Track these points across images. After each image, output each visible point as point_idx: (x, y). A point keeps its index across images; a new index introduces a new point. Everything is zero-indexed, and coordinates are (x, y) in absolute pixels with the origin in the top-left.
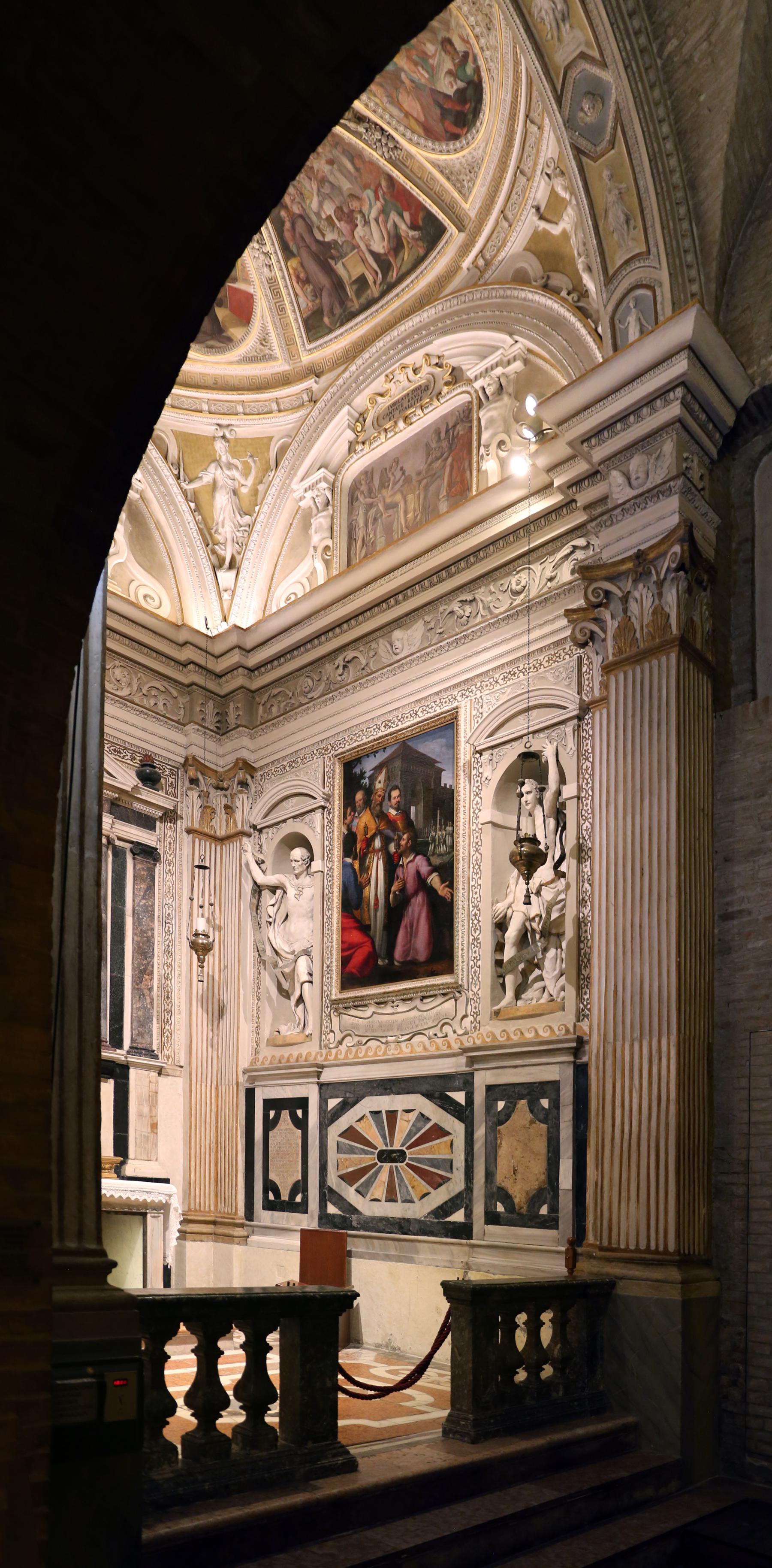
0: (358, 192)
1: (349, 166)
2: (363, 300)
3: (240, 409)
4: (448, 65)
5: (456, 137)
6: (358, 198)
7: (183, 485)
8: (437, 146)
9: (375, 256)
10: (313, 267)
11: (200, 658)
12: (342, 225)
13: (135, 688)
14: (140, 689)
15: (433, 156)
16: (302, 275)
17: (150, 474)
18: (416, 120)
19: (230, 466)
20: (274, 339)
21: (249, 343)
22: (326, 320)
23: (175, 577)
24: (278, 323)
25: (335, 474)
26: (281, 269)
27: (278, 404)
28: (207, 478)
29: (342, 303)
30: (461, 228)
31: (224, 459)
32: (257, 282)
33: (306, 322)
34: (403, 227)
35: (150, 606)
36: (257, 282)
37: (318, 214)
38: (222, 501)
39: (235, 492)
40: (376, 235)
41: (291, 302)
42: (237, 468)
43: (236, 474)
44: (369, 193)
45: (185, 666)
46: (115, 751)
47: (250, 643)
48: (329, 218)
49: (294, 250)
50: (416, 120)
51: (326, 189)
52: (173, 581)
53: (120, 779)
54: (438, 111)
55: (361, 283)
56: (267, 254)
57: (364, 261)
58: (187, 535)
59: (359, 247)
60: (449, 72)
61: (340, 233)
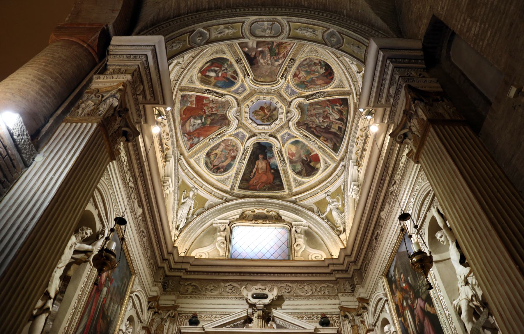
0: (324, 110)
1: (318, 106)
2: (343, 132)
3: (328, 184)
4: (319, 67)
5: (333, 78)
6: (325, 111)
7: (321, 216)
8: (331, 84)
9: (338, 120)
10: (326, 135)
11: (336, 268)
12: (327, 120)
13: (314, 290)
14: (316, 290)
15: (331, 87)
16: (325, 139)
17: (309, 219)
18: (323, 84)
19: (333, 202)
20: (328, 160)
21: (322, 165)
22: (338, 145)
23: (326, 246)
24: (327, 155)
25: (358, 182)
26: (319, 142)
27: (337, 176)
28: (328, 210)
29: (339, 137)
30: (349, 94)
31: (331, 201)
32: (316, 150)
33: (333, 149)
34: (339, 107)
35: (318, 259)
36: (316, 150)
37: (320, 123)
38: (334, 213)
39: (337, 209)
40: (335, 115)
41: (327, 148)
42: (335, 201)
43: (336, 203)
44: (327, 108)
45: (332, 273)
46: (308, 318)
47: (349, 252)
48: (323, 121)
49: (320, 135)
50: (323, 84)
51: (318, 116)
52: (326, 247)
53: (308, 328)
54: (325, 77)
55: (340, 128)
56: (314, 141)
57: (337, 123)
58: (327, 230)
59: (333, 121)
60: (320, 68)
61: (327, 122)
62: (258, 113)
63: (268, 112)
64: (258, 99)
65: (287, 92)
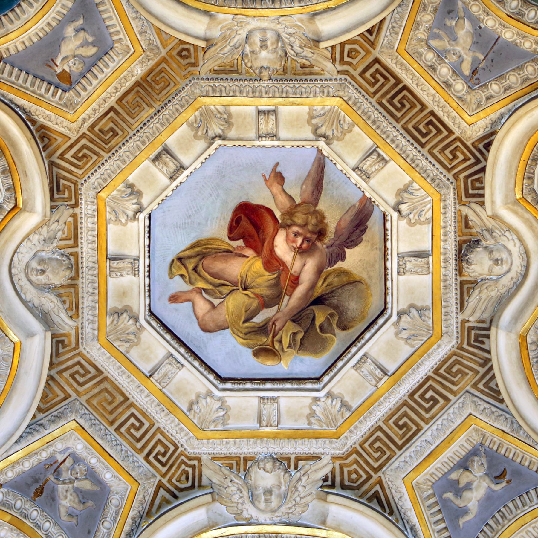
62: (218, 266)
63: (301, 251)
64: (216, 129)
65: (441, 55)
